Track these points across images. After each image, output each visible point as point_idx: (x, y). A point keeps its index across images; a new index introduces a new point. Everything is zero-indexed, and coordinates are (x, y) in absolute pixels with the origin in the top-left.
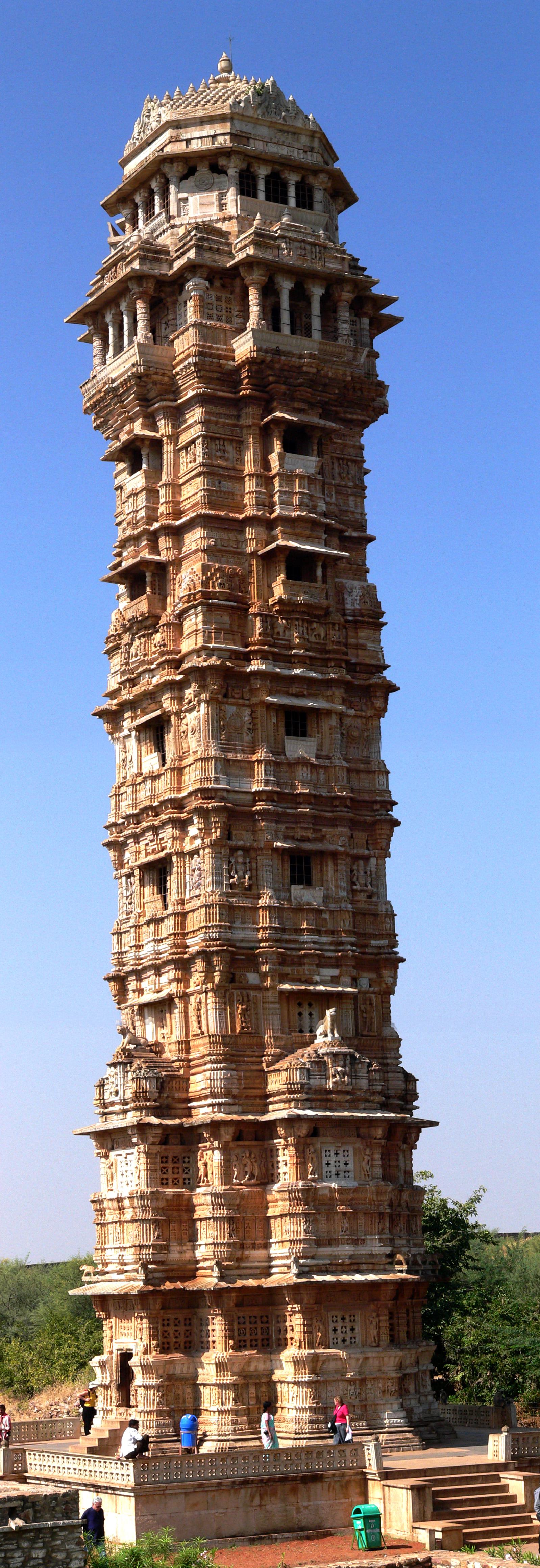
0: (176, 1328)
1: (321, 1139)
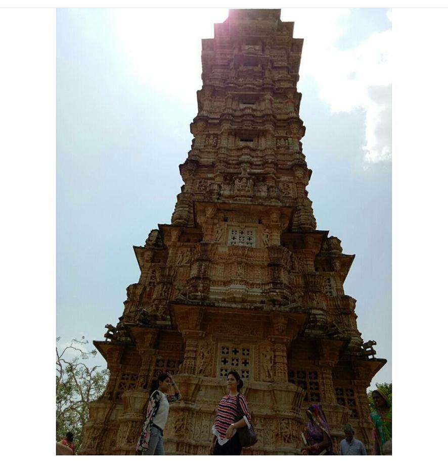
0: (132, 382)
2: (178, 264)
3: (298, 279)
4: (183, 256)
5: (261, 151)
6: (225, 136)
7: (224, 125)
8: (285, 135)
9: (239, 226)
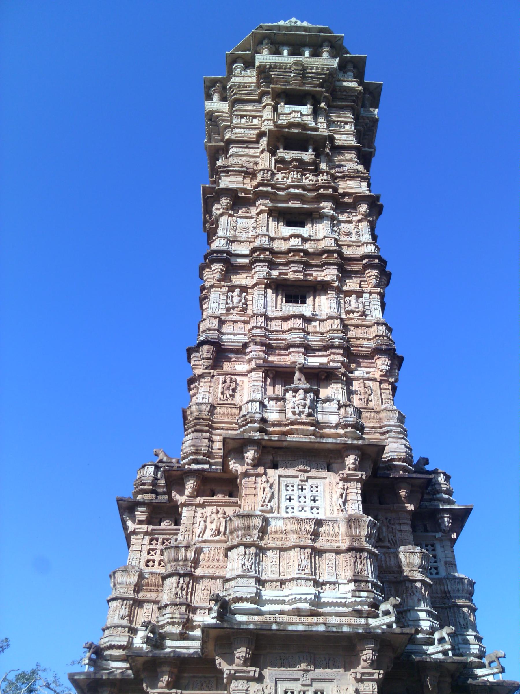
1: (281, 471)
2: (199, 537)
3: (388, 559)
4: (205, 521)
5: (322, 321)
6: (258, 292)
7: (258, 268)
8: (358, 289)
9: (297, 477)
